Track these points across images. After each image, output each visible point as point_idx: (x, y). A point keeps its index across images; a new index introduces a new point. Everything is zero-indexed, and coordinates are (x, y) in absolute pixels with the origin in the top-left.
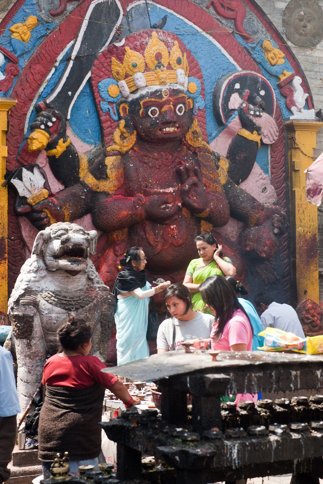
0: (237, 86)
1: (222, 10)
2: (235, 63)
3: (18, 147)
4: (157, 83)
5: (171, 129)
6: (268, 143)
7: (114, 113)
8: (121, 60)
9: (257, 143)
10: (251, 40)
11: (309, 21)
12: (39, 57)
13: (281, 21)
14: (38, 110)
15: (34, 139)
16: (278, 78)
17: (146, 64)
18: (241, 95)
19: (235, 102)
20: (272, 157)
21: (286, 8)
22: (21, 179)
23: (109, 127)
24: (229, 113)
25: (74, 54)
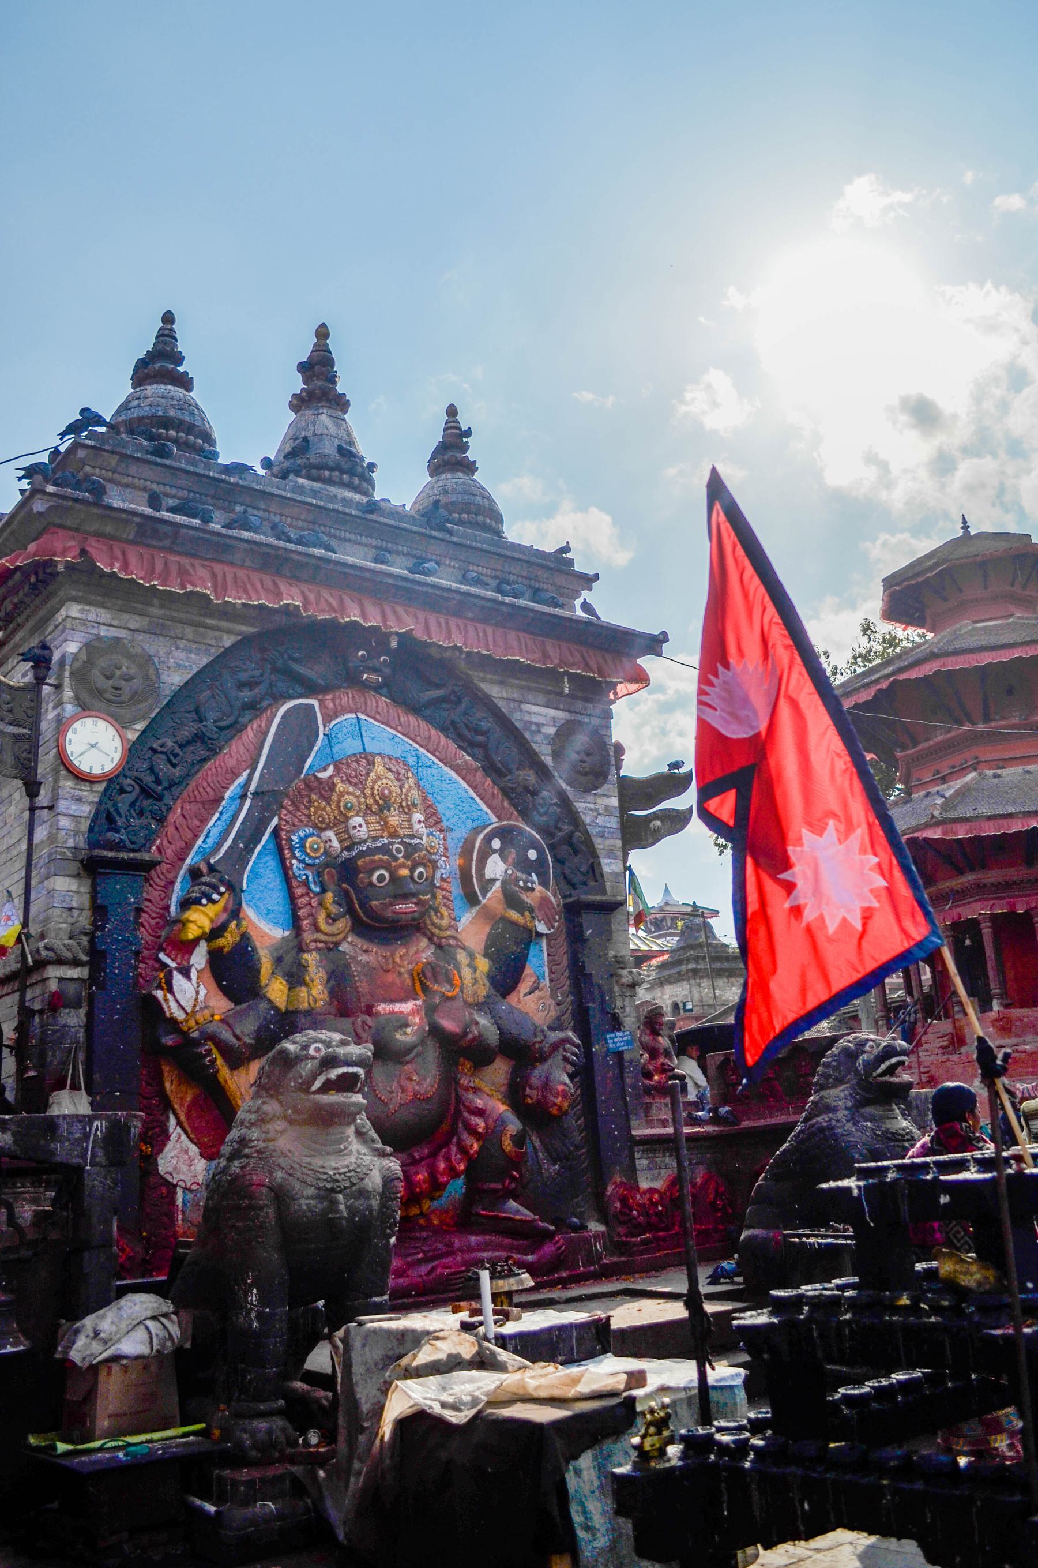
0: (496, 844)
1: (466, 733)
2: (489, 811)
3: (159, 937)
4: (386, 834)
7: (315, 882)
8: (328, 800)
12: (196, 793)
13: (550, 752)
14: (195, 874)
15: (192, 922)
17: (367, 805)
18: (503, 859)
19: (496, 868)
20: (549, 955)
21: (557, 734)
22: (170, 990)
23: (306, 905)
24: (487, 884)
25: (252, 788)
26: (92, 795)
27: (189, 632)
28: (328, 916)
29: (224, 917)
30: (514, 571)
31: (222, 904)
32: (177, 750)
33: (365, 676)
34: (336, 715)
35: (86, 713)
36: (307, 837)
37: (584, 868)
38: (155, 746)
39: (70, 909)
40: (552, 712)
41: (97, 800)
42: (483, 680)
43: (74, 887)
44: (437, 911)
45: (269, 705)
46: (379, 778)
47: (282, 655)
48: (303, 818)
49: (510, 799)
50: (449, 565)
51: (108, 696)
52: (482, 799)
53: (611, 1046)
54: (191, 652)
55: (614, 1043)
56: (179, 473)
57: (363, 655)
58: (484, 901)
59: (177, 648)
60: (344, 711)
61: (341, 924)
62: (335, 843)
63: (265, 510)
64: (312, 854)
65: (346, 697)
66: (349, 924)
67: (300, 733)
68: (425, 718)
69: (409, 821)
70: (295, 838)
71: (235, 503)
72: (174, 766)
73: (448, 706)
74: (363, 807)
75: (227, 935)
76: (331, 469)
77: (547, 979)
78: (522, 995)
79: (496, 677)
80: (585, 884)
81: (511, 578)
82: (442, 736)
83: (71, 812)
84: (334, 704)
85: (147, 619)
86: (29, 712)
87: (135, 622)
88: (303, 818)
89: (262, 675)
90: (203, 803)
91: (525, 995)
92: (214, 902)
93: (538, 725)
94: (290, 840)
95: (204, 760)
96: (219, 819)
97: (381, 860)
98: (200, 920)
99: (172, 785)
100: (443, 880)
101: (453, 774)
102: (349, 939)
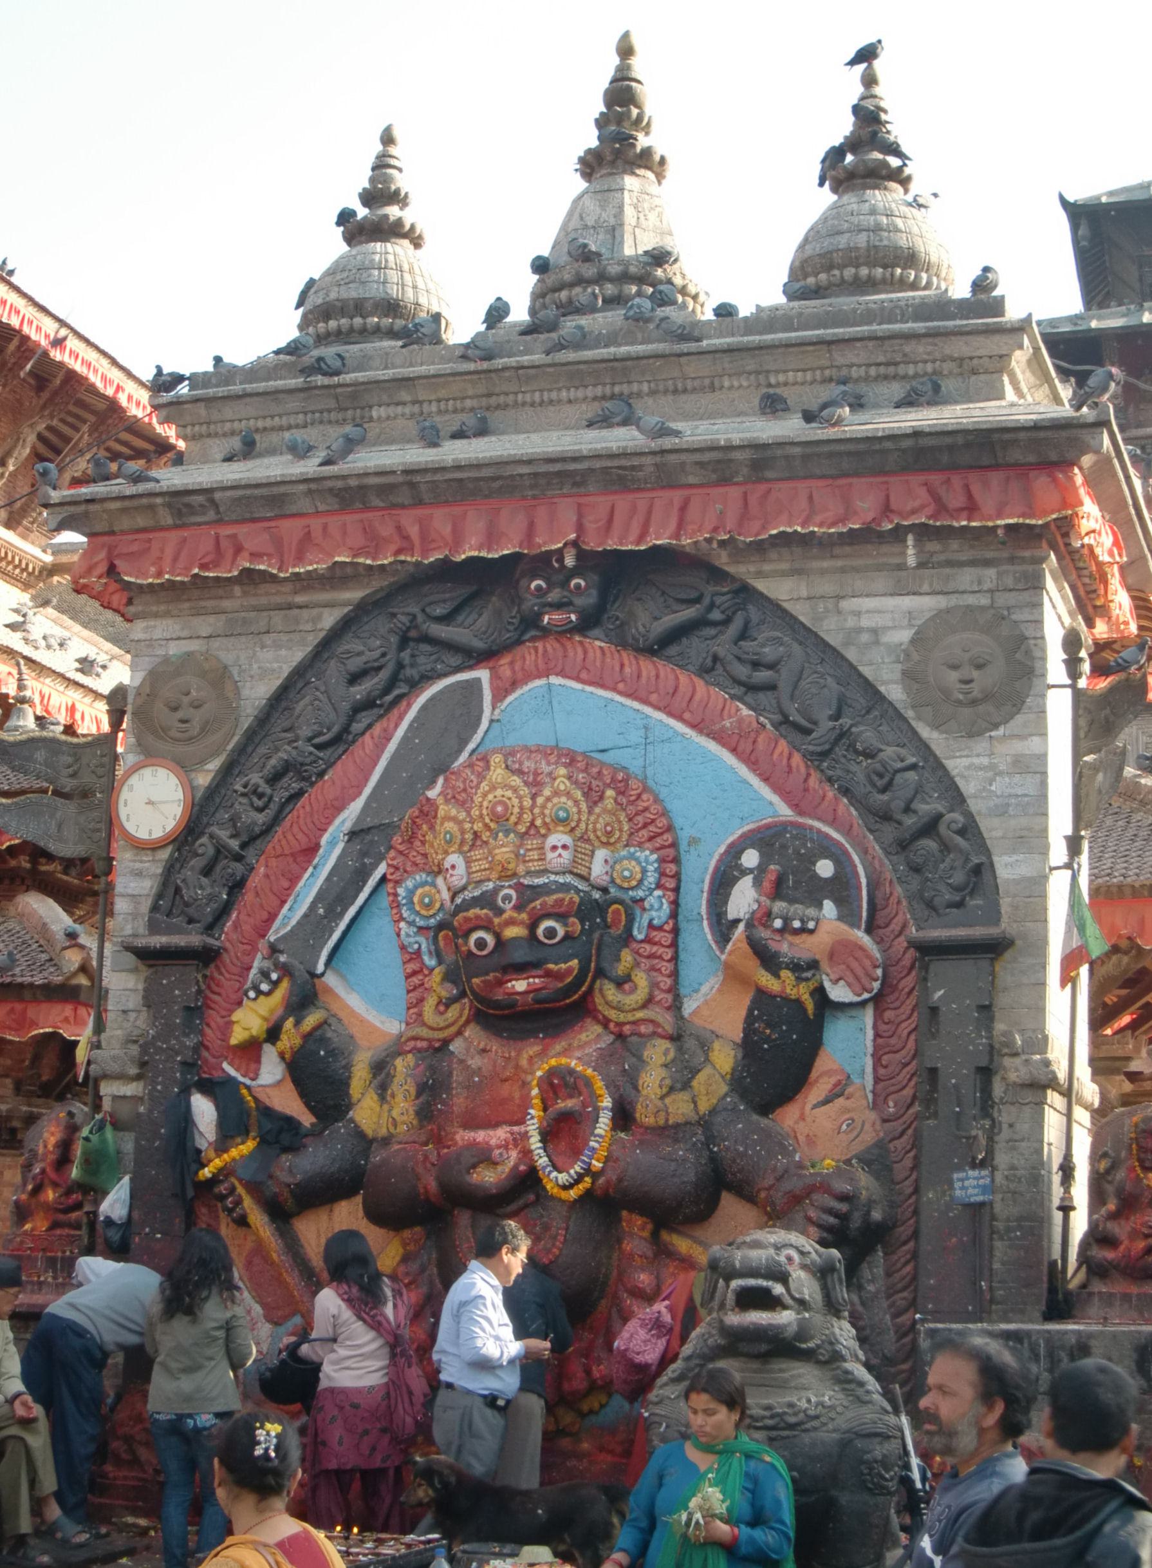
0: (751, 858)
1: (742, 671)
2: (775, 799)
5: (520, 986)
6: (847, 1000)
7: (430, 953)
9: (798, 1002)
10: (814, 735)
11: (979, 667)
13: (897, 676)
16: (899, 823)
17: (475, 833)
20: (877, 1035)
21: (913, 641)
25: (348, 826)
26: (154, 866)
27: (277, 618)
29: (280, 1012)
30: (855, 360)
32: (264, 788)
33: (546, 619)
34: (514, 684)
35: (154, 760)
36: (416, 888)
37: (958, 878)
38: (238, 787)
39: (124, 1012)
40: (907, 602)
41: (160, 871)
42: (760, 574)
43: (131, 985)
45: (400, 697)
46: (493, 788)
47: (414, 617)
48: (419, 859)
49: (818, 768)
50: (731, 388)
51: (174, 733)
52: (766, 780)
53: (958, 1193)
54: (280, 647)
55: (963, 1188)
56: (281, 396)
57: (539, 588)
59: (262, 647)
60: (529, 677)
61: (452, 1013)
62: (446, 895)
63: (414, 402)
64: (423, 912)
65: (529, 654)
66: (466, 1012)
68: (668, 659)
69: (541, 848)
70: (401, 891)
71: (371, 407)
72: (260, 810)
73: (712, 631)
74: (469, 836)
75: (284, 1037)
76: (572, 285)
78: (808, 1107)
79: (785, 566)
80: (959, 905)
81: (855, 373)
82: (700, 683)
83: (130, 891)
84: (514, 672)
85: (223, 617)
86: (100, 771)
87: (205, 625)
88: (419, 859)
89: (384, 655)
90: (292, 855)
91: (815, 1107)
92: (268, 994)
93: (875, 631)
94: (396, 895)
95: (300, 794)
96: (312, 875)
97: (477, 917)
98: (249, 1021)
99: (253, 839)
100: (651, 926)
101: (712, 746)
102: (467, 1034)
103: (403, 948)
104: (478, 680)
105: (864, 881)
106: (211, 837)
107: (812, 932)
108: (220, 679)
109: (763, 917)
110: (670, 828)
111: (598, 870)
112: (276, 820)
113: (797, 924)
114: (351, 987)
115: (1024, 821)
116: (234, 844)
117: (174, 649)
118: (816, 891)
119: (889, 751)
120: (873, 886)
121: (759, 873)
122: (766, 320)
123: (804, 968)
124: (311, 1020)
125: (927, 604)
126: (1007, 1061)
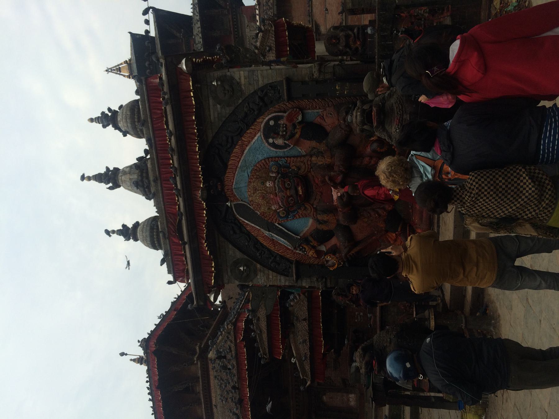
0: (271, 140)
11: (225, 88)
19: (280, 142)
20: (309, 109)
28: (304, 210)
31: (305, 246)
37: (272, 92)
40: (211, 107)
44: (299, 168)
52: (253, 138)
58: (292, 146)
67: (243, 209)
77: (320, 111)
92: (305, 249)
95: (261, 244)
98: (311, 253)
101: (246, 151)
103: (293, 219)
104: (234, 205)
105: (274, 114)
106: (271, 263)
107: (286, 125)
108: (237, 263)
109: (283, 137)
110: (264, 160)
111: (274, 175)
112: (267, 248)
113: (284, 129)
114: (302, 231)
115: (259, 76)
116: (272, 258)
117: (229, 274)
118: (277, 125)
119: (245, 109)
120: (275, 112)
121: (273, 138)
122: (149, 142)
123: (294, 126)
124: (311, 239)
125: (211, 102)
126: (314, 77)
